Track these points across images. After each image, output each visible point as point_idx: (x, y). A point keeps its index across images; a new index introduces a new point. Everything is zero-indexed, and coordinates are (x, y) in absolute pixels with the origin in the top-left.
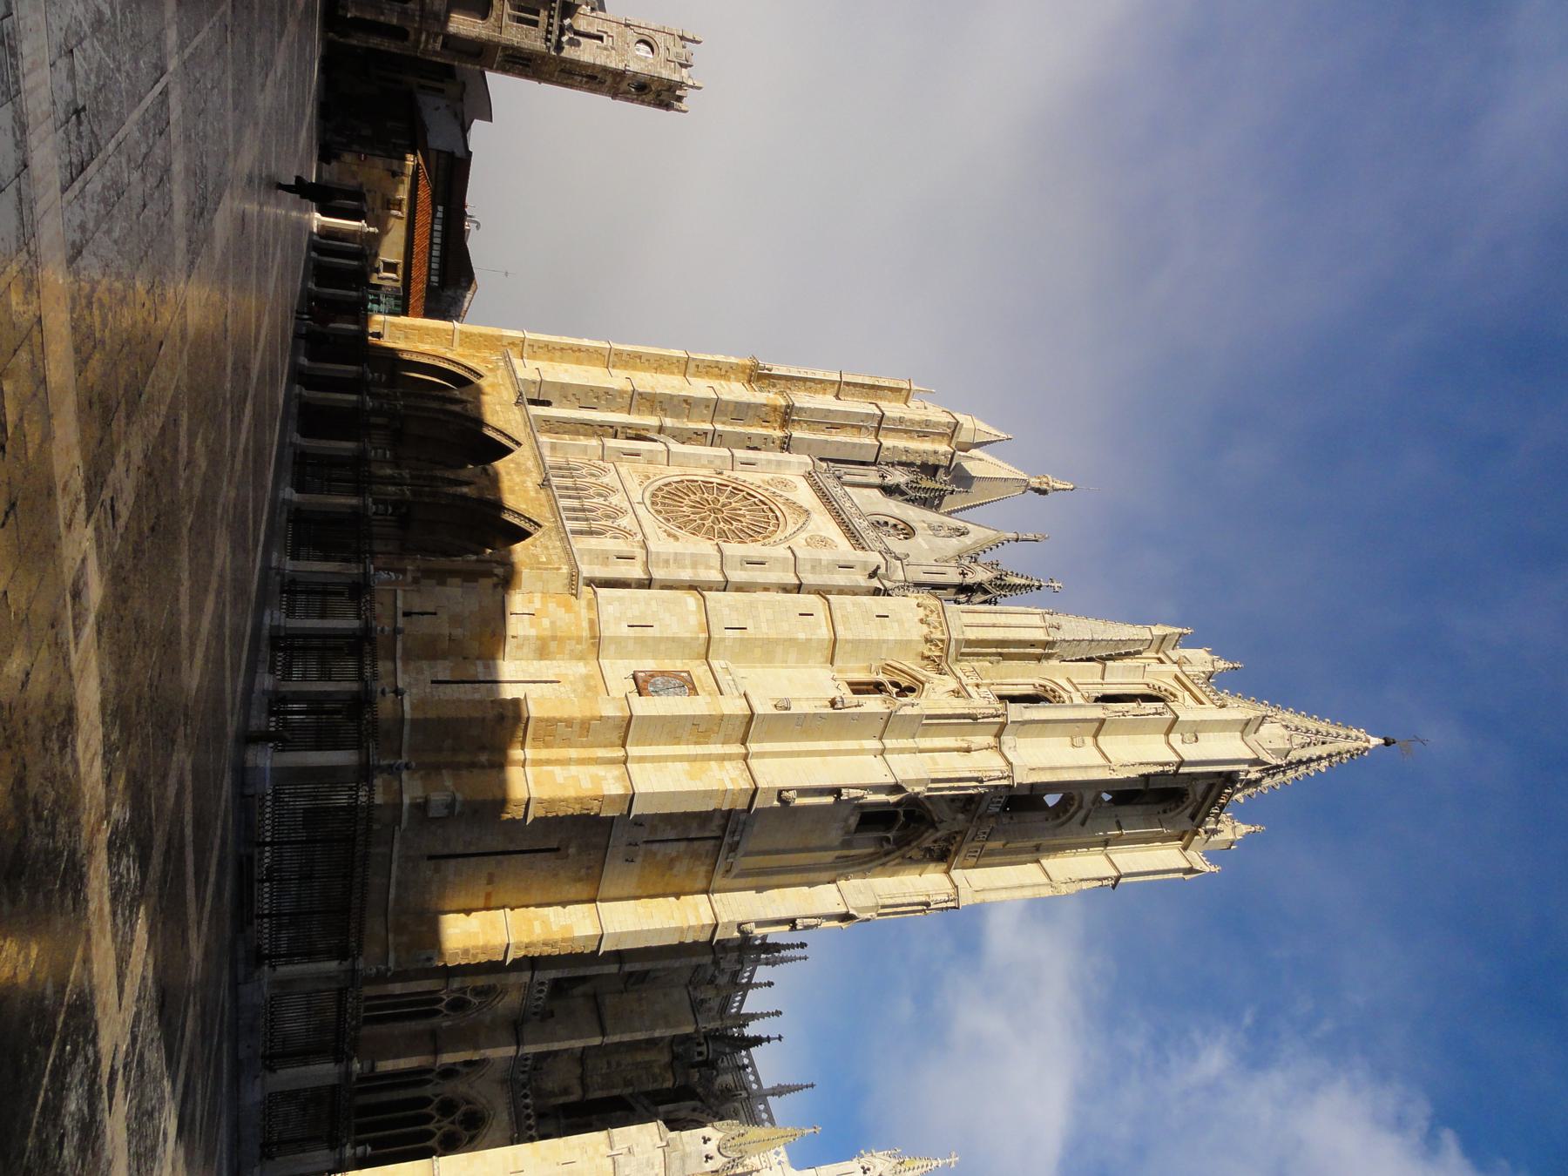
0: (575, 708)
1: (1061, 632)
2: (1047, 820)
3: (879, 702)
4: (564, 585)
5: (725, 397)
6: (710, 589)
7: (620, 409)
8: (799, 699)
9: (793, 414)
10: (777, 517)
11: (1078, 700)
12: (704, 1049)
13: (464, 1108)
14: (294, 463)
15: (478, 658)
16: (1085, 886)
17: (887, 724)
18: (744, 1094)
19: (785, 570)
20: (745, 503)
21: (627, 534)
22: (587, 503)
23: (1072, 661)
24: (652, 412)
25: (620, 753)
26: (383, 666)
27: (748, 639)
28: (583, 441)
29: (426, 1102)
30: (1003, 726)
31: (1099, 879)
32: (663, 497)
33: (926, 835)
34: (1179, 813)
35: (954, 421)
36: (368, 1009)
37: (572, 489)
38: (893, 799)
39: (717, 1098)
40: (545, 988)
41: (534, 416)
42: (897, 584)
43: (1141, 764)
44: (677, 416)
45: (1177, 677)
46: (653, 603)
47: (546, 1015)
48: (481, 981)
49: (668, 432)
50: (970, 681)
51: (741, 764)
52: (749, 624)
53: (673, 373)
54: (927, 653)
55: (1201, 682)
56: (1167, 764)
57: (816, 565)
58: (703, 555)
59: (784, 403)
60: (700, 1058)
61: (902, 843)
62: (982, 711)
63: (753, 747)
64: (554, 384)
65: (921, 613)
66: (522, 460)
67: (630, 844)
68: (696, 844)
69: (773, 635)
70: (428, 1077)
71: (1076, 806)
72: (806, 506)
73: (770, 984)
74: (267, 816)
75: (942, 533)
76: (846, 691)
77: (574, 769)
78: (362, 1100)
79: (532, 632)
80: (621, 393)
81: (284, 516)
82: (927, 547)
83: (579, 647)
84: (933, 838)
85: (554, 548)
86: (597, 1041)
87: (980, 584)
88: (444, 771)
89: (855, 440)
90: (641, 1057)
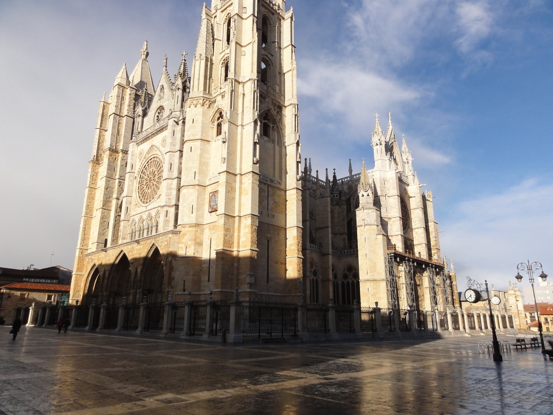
1: (202, 54)
2: (270, 69)
3: (225, 125)
5: (105, 174)
6: (180, 184)
7: (109, 214)
9: (113, 148)
10: (154, 158)
11: (228, 51)
12: (335, 195)
13: (346, 272)
14: (127, 330)
15: (201, 266)
16: (294, 58)
17: (232, 123)
18: (350, 182)
19: (174, 156)
20: (148, 169)
21: (158, 213)
22: (146, 227)
23: (213, 51)
24: (111, 202)
25: (237, 218)
26: (202, 298)
27: (199, 171)
28: (121, 228)
29: (343, 283)
30: (236, 80)
31: (292, 52)
32: (144, 199)
33: (272, 113)
34: (271, 19)
36: (314, 302)
37: (140, 232)
38: (259, 124)
39: (350, 192)
40: (312, 245)
41: (111, 245)
42: (181, 114)
43: (253, 31)
44: (112, 193)
45: (222, 12)
47: (321, 245)
48: (308, 265)
49: (119, 196)
50: (219, 91)
51: (243, 176)
53: (95, 193)
54: (208, 106)
55: (224, 2)
56: (253, 20)
57: (173, 144)
58: (167, 186)
59: (109, 151)
60: (338, 196)
61: (274, 122)
62: (230, 88)
63: (238, 172)
64: (98, 238)
65: (192, 106)
67: (268, 216)
68: (270, 194)
69: (198, 162)
70: (336, 282)
71: (266, 57)
72: (150, 146)
73: (317, 171)
74: (250, 335)
75: (162, 95)
78: (341, 302)
79: (193, 247)
80: (103, 213)
81: (147, 333)
82: (167, 102)
83: (199, 231)
84: (274, 111)
85: (162, 239)
86: (330, 229)
87: (183, 83)
89: (124, 125)
90: (336, 216)
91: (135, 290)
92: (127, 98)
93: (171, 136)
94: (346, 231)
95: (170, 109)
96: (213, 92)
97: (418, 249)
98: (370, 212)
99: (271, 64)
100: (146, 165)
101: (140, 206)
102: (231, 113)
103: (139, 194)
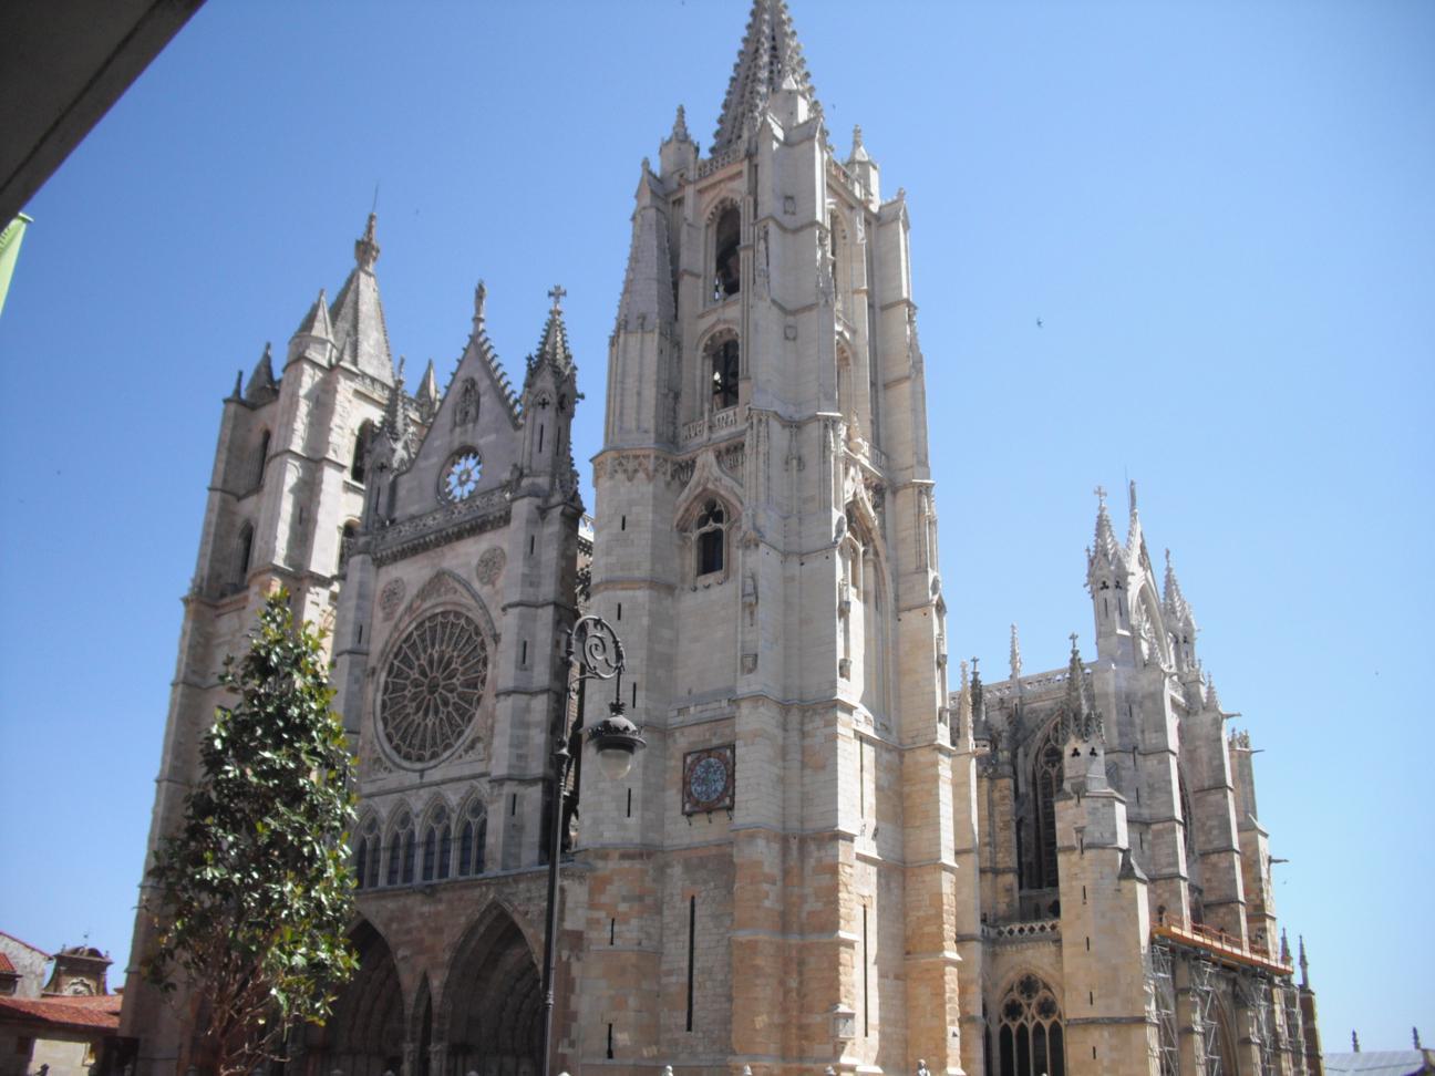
3: (748, 552)
4: (581, 883)
11: (733, 312)
13: (1015, 995)
22: (419, 837)
23: (676, 308)
29: (1005, 1031)
32: (410, 745)
39: (1017, 730)
46: (601, 785)
54: (669, 478)
57: (531, 581)
75: (472, 410)
76: (711, 578)
77: (808, 890)
79: (634, 922)
82: (492, 437)
85: (529, 891)
87: (558, 388)
91: (418, 1044)
93: (525, 554)
95: (515, 466)
96: (683, 432)
97: (1219, 920)
98: (1099, 805)
99: (851, 361)
100: (411, 633)
101: (393, 768)
103: (386, 725)
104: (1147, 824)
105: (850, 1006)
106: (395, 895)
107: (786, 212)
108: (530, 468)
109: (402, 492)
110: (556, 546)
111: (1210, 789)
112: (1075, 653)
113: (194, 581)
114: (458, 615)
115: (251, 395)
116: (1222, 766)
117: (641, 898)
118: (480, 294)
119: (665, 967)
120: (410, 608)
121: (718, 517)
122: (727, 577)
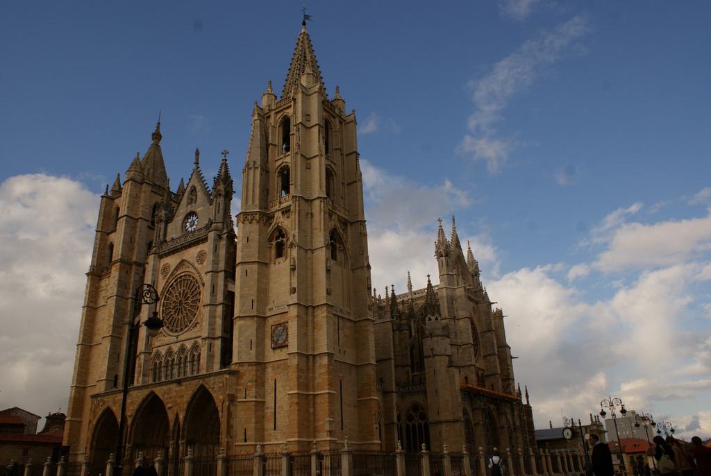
0: (293, 375)
2: (333, 180)
5: (115, 291)
8: (291, 283)
10: (184, 276)
11: (288, 159)
13: (411, 412)
15: (264, 412)
19: (217, 277)
21: (196, 347)
28: (141, 360)
29: (408, 426)
35: (130, 182)
52: (251, 298)
56: (319, 131)
57: (215, 262)
61: (341, 242)
64: (108, 374)
66: (163, 391)
69: (255, 289)
72: (179, 261)
75: (194, 198)
76: (280, 260)
77: (317, 375)
79: (254, 390)
82: (202, 208)
85: (215, 380)
86: (393, 361)
87: (225, 189)
88: (316, 424)
91: (175, 441)
92: (143, 195)
94: (409, 363)
102: (299, 236)
104: (460, 345)
105: (333, 418)
106: (166, 383)
107: (307, 121)
108: (215, 220)
109: (169, 230)
110: (225, 249)
111: (486, 331)
112: (429, 281)
113: (91, 267)
114: (189, 276)
115: (113, 194)
116: (491, 322)
117: (256, 381)
118: (197, 154)
119: (266, 406)
120: (172, 275)
121: (283, 237)
122: (286, 259)
